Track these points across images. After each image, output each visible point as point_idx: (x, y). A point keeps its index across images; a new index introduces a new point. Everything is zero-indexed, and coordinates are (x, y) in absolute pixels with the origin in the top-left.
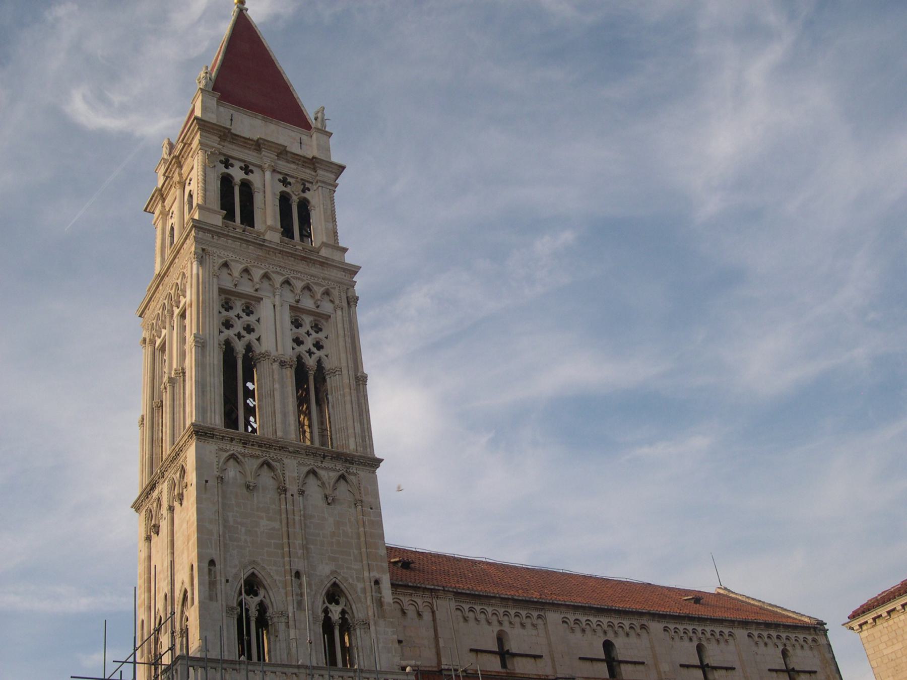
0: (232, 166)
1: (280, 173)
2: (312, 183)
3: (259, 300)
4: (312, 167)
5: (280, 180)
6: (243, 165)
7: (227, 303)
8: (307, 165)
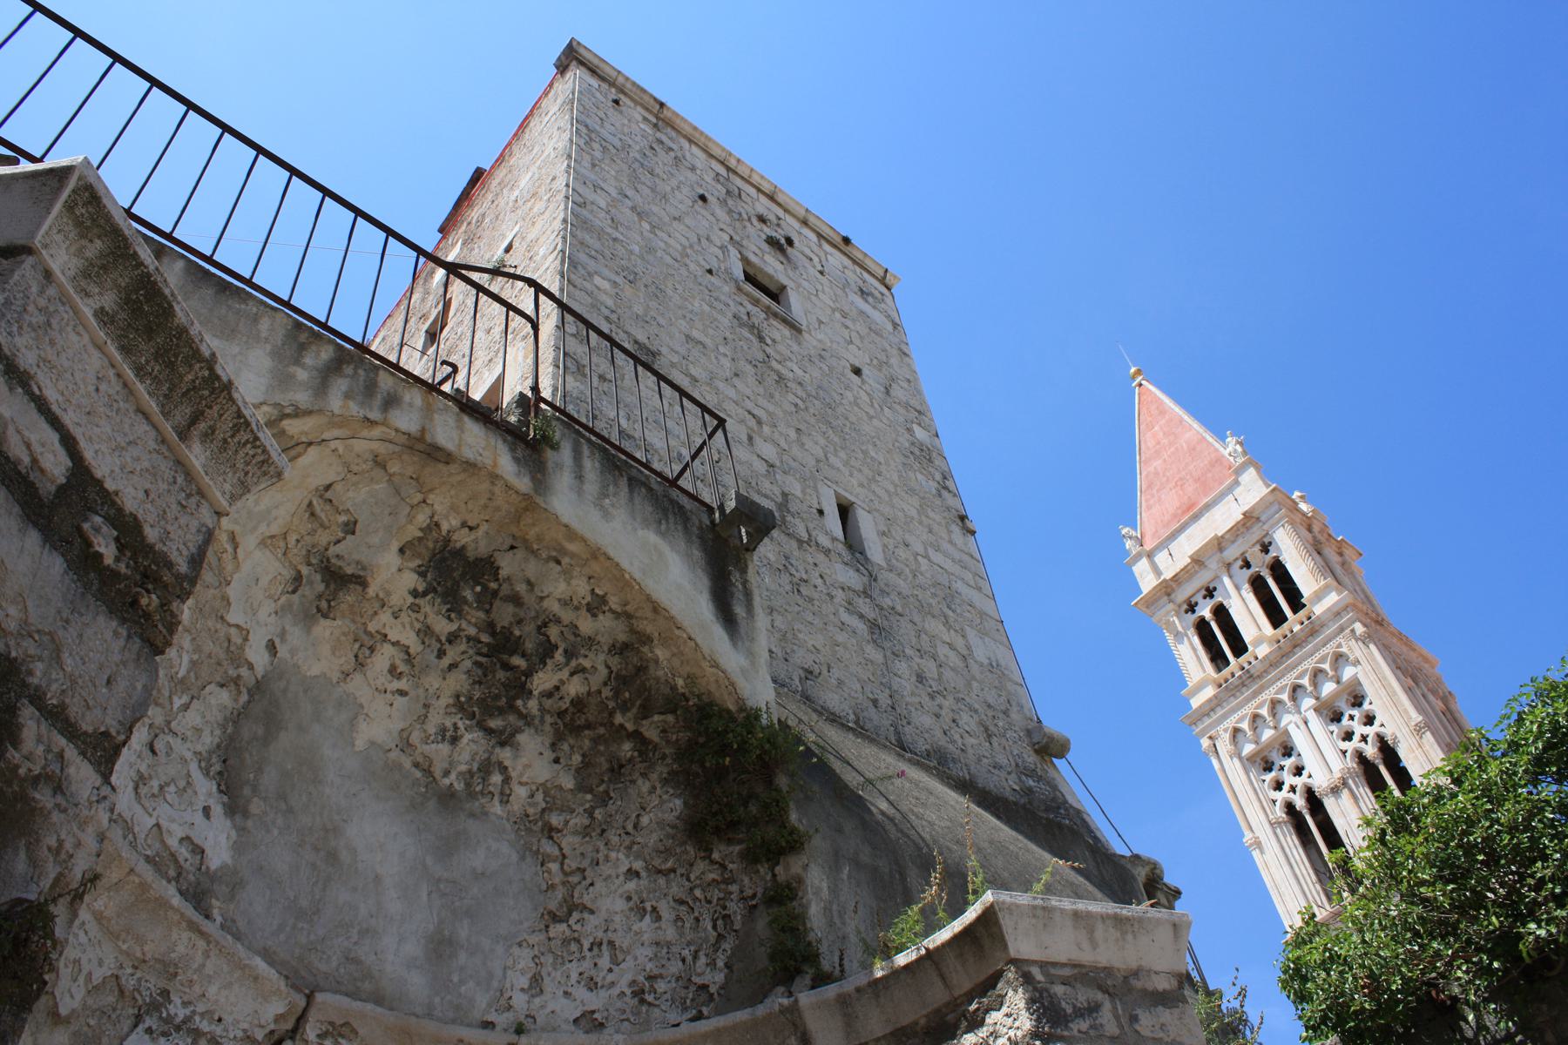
0: (1196, 604)
1: (1237, 559)
2: (1267, 534)
3: (1286, 733)
4: (1254, 520)
5: (1242, 568)
6: (1204, 592)
7: (1267, 762)
8: (1248, 524)
